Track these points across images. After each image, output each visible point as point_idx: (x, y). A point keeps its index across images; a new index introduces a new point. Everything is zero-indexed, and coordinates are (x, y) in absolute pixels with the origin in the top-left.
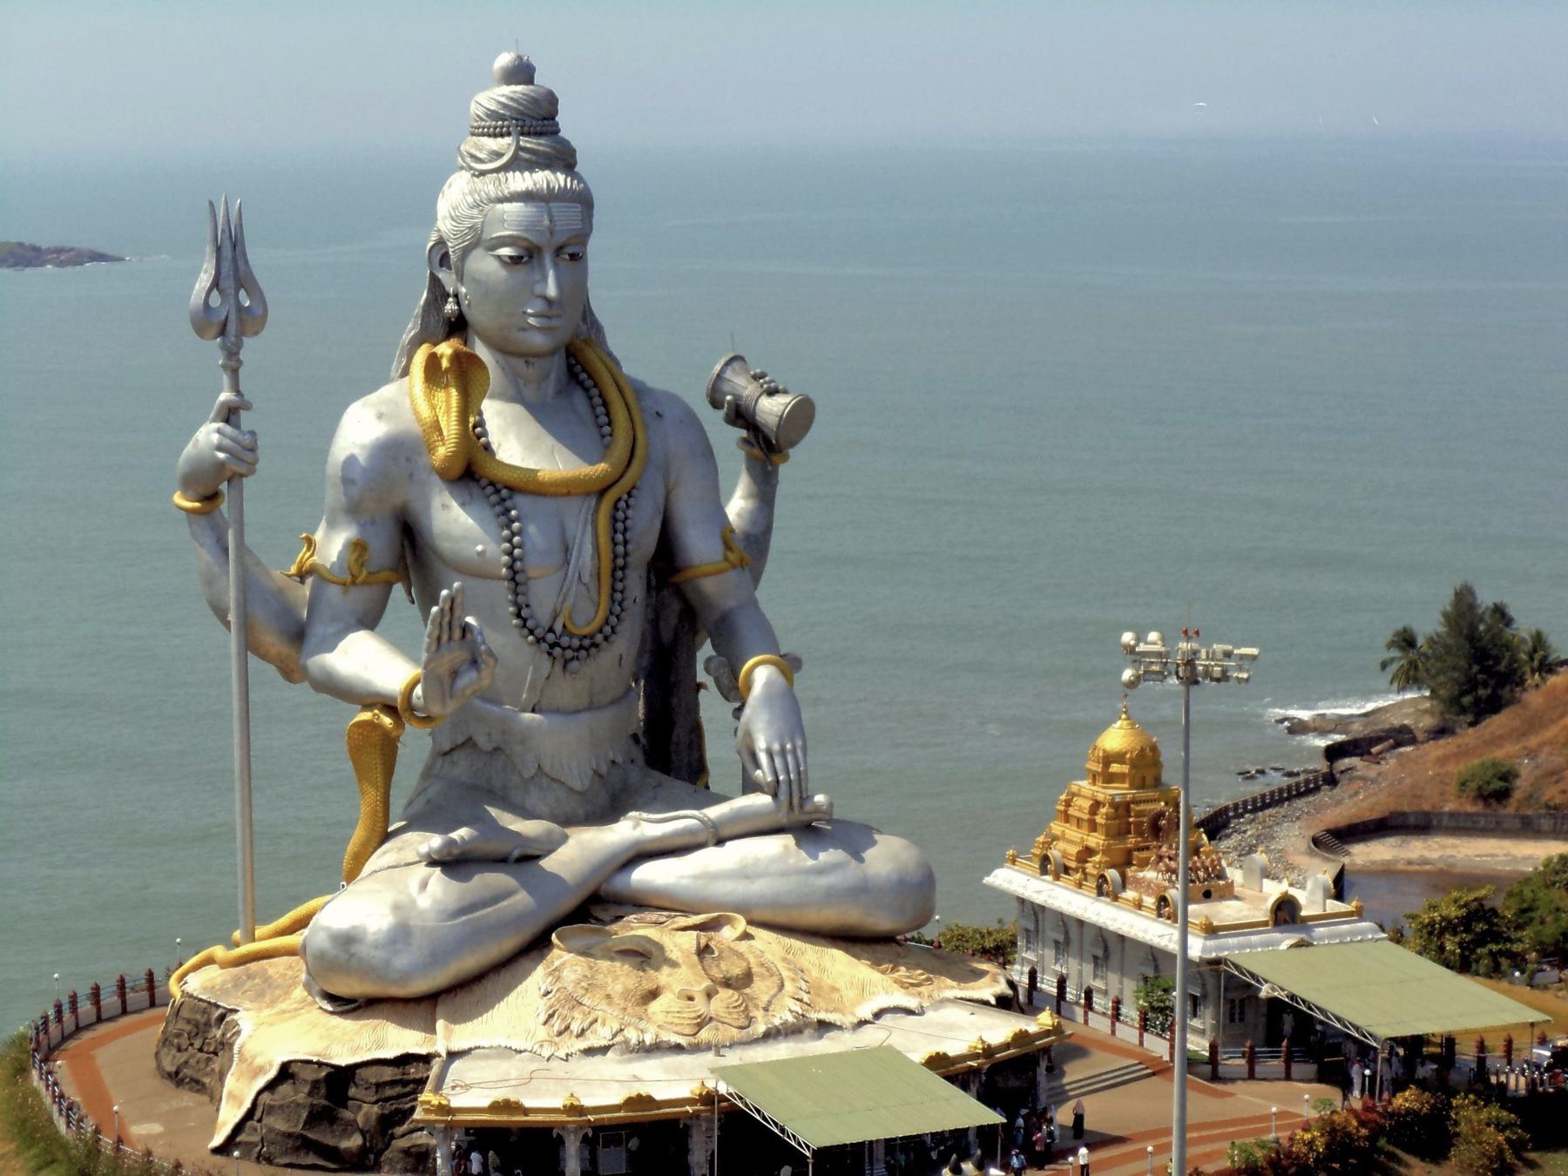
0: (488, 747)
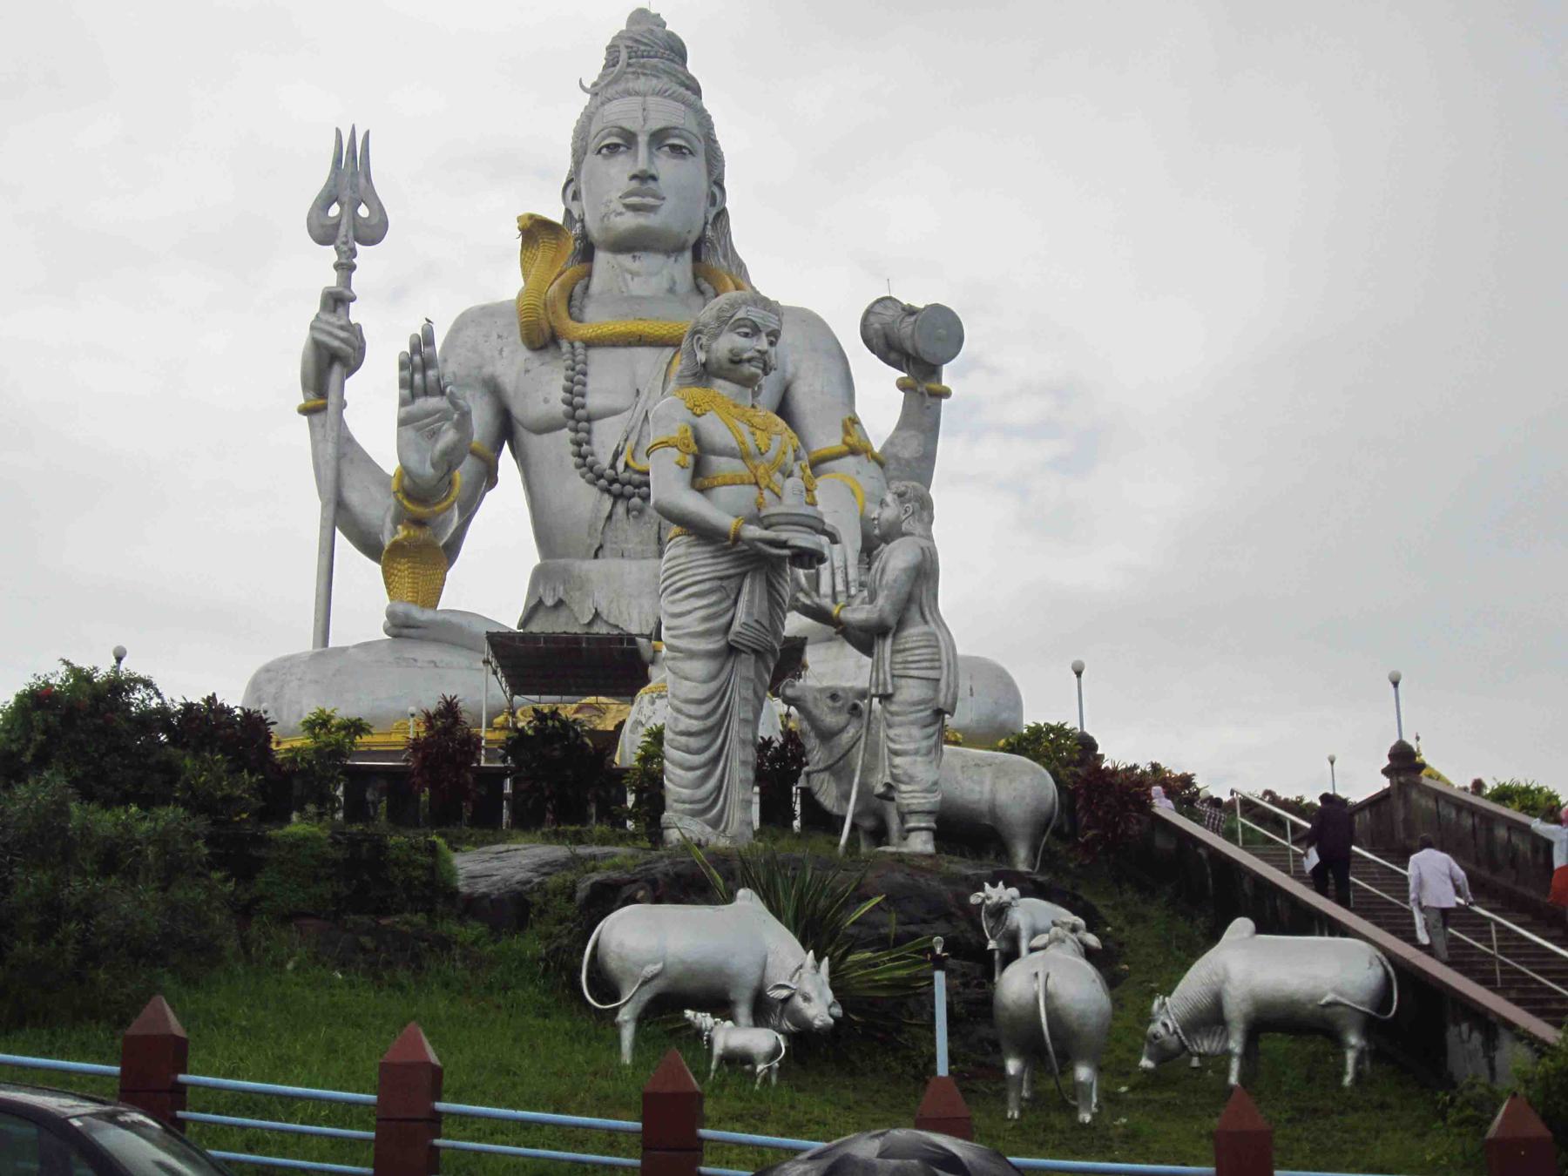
0: (549, 602)
